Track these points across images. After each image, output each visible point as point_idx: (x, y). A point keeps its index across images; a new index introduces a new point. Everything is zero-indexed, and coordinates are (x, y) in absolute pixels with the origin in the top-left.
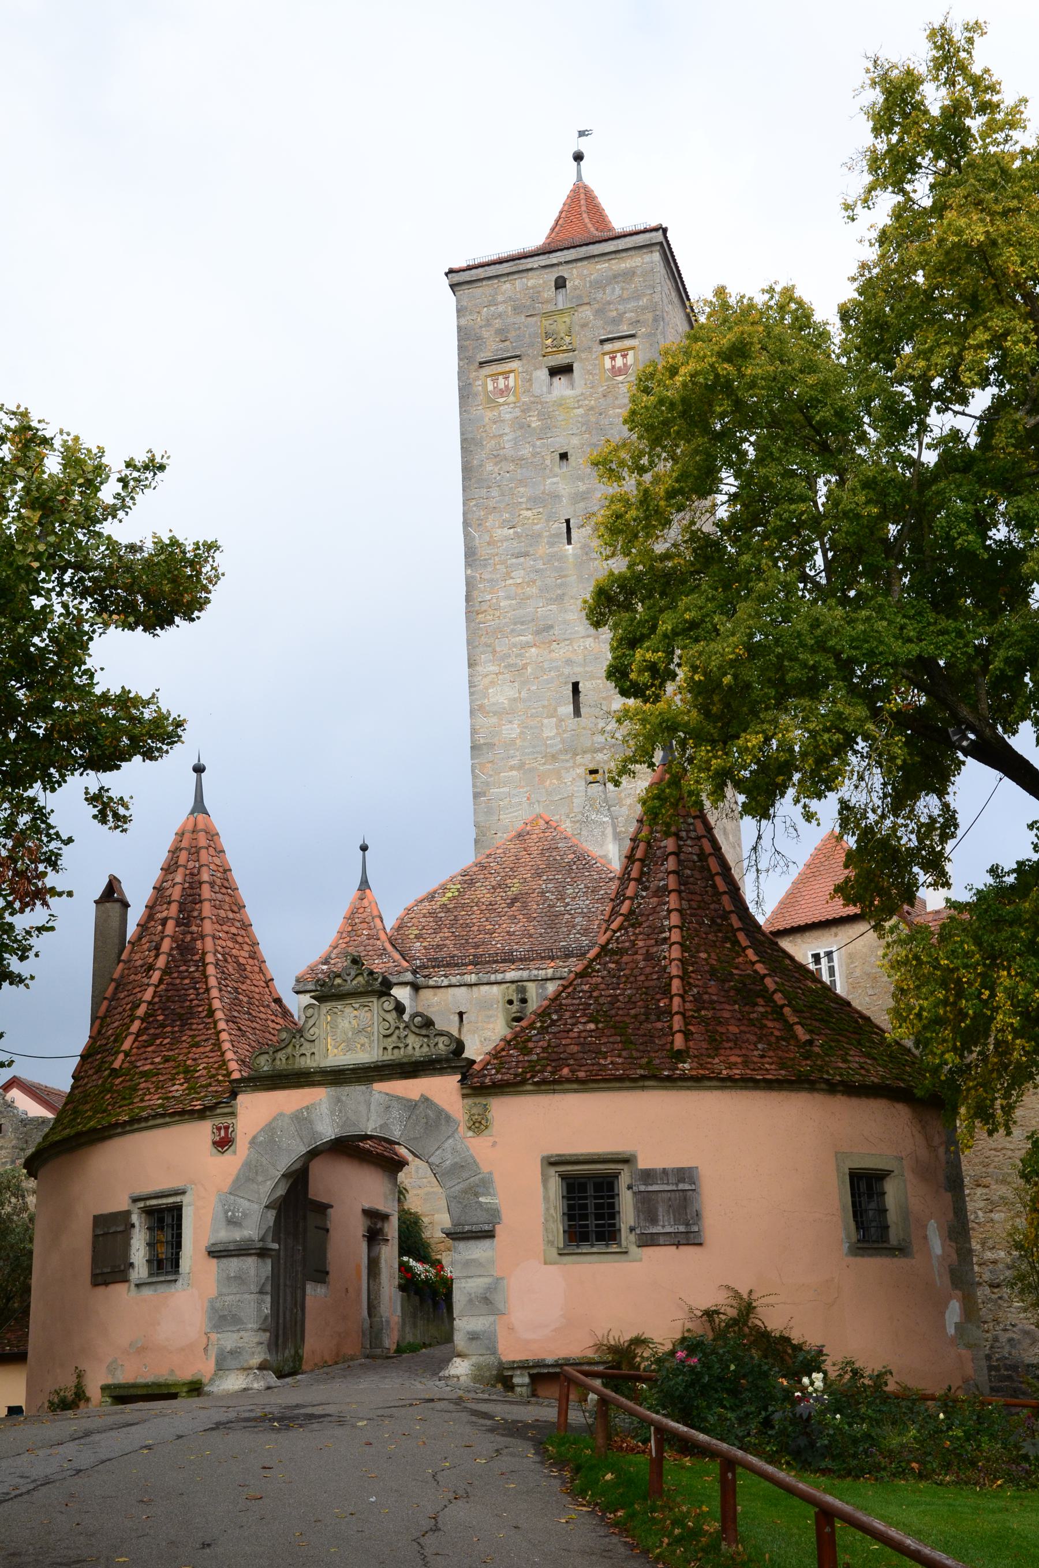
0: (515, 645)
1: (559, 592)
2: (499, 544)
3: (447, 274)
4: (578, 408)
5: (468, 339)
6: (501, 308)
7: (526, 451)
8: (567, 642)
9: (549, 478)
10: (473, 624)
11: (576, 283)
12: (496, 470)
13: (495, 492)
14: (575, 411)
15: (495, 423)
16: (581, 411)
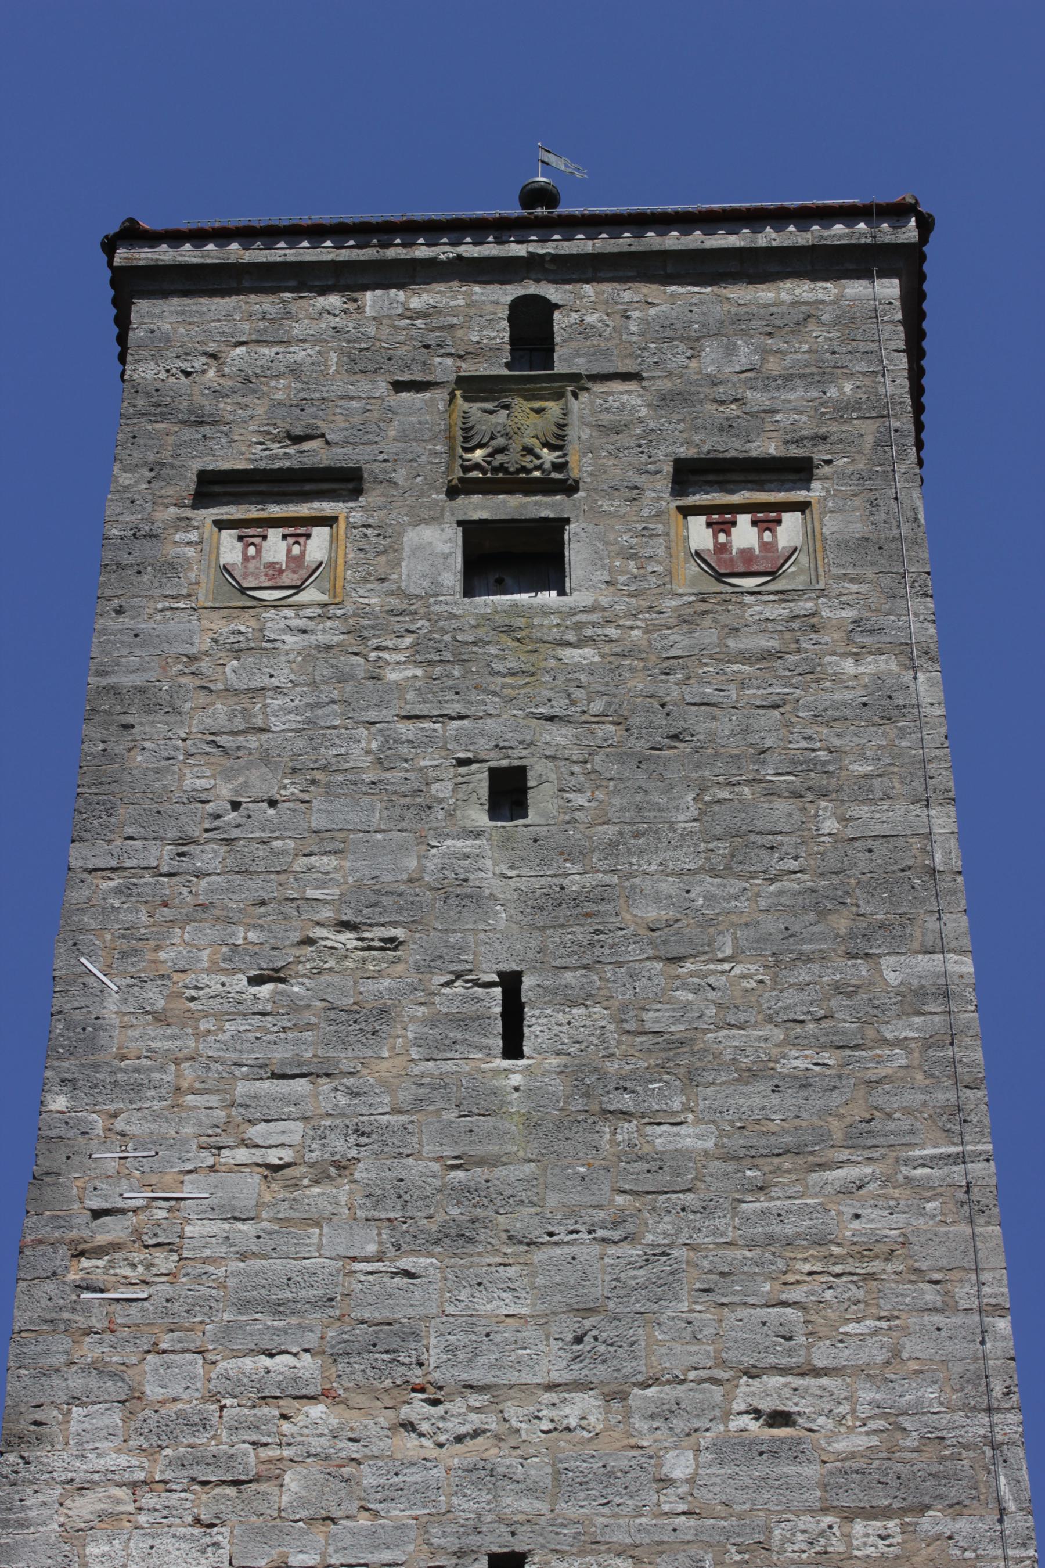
0: (235, 1387)
1: (455, 1211)
2: (204, 1025)
3: (109, 246)
4: (578, 645)
5: (163, 417)
6: (299, 354)
7: (356, 750)
8: (476, 1400)
9: (442, 836)
10: (50, 1287)
11: (591, 319)
12: (225, 791)
13: (209, 856)
14: (566, 653)
15: (237, 653)
16: (587, 655)
